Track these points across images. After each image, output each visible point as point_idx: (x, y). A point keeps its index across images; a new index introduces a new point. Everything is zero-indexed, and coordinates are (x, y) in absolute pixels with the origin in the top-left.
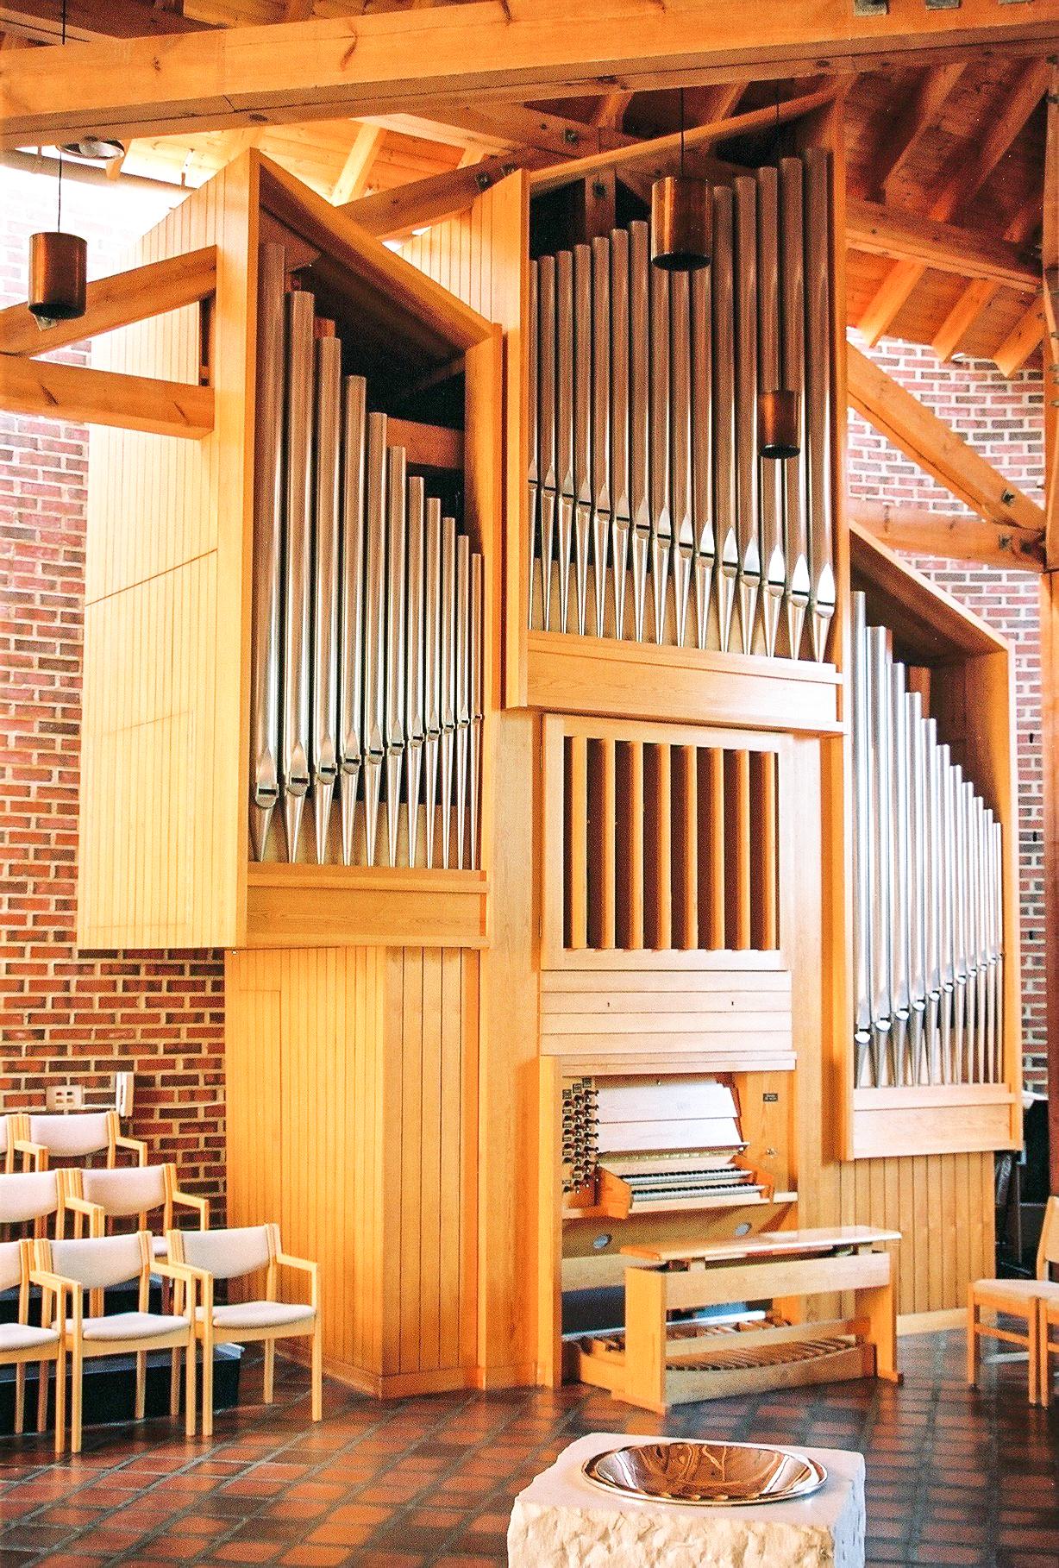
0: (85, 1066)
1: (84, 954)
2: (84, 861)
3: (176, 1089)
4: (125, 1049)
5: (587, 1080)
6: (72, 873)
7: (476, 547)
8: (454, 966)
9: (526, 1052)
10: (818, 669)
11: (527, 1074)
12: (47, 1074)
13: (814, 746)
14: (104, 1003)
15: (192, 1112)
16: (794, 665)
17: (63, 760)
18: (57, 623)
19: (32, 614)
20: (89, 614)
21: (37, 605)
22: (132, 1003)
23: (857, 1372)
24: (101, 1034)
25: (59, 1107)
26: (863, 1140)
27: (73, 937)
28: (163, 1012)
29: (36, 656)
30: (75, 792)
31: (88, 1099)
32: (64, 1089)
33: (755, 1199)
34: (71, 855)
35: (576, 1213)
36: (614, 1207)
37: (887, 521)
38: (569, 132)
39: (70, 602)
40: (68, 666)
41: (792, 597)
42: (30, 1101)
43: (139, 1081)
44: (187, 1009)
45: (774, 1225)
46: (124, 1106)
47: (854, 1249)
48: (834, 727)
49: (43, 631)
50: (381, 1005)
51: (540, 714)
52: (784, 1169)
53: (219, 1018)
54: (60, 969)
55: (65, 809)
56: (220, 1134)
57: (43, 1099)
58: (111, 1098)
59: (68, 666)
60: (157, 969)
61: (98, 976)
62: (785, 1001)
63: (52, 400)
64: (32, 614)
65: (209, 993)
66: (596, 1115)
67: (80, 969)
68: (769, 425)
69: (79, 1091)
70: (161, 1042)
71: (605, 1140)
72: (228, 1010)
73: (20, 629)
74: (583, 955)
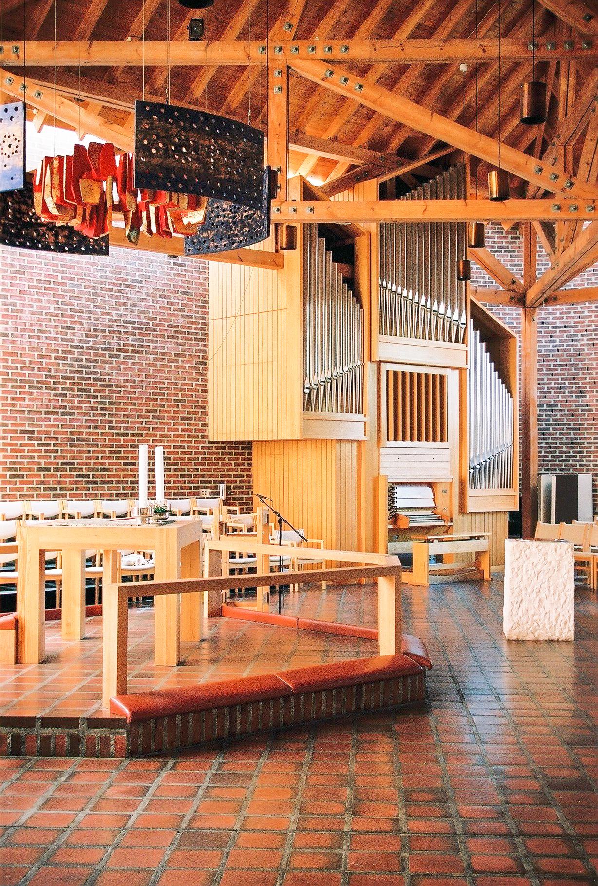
0: (210, 482)
1: (210, 442)
2: (210, 410)
3: (237, 491)
4: (222, 476)
5: (393, 483)
6: (206, 414)
7: (361, 307)
8: (354, 445)
9: (376, 474)
10: (460, 345)
11: (376, 481)
12: (200, 485)
13: (457, 372)
14: (216, 459)
15: (242, 499)
16: (453, 345)
17: (202, 374)
18: (200, 326)
19: (192, 323)
20: (211, 323)
21: (194, 320)
22: (224, 459)
23: (478, 578)
24: (215, 470)
25: (203, 496)
26: (471, 507)
27: (208, 437)
28: (233, 462)
29: (194, 337)
30: (206, 385)
31: (212, 493)
32: (204, 490)
33: (443, 523)
34: (205, 408)
35: (391, 527)
36: (402, 525)
37: (476, 291)
38: (382, 157)
39: (203, 318)
40: (203, 340)
41: (461, 325)
42: (195, 494)
43: (228, 488)
44: (240, 461)
45: (446, 532)
46: (223, 496)
47: (479, 537)
48: (465, 366)
49: (196, 329)
50: (334, 458)
51: (379, 363)
52: (449, 514)
53: (250, 465)
54: (203, 448)
55: (203, 391)
56: (250, 506)
57: (198, 494)
58: (218, 493)
59: (203, 340)
60: (231, 448)
61: (214, 450)
62: (448, 458)
63: (241, 260)
64: (192, 323)
65: (247, 456)
66: (396, 495)
67: (209, 448)
68: (461, 271)
69: (208, 491)
70: (232, 473)
71: (399, 504)
72: (254, 462)
73: (189, 328)
74: (392, 443)
